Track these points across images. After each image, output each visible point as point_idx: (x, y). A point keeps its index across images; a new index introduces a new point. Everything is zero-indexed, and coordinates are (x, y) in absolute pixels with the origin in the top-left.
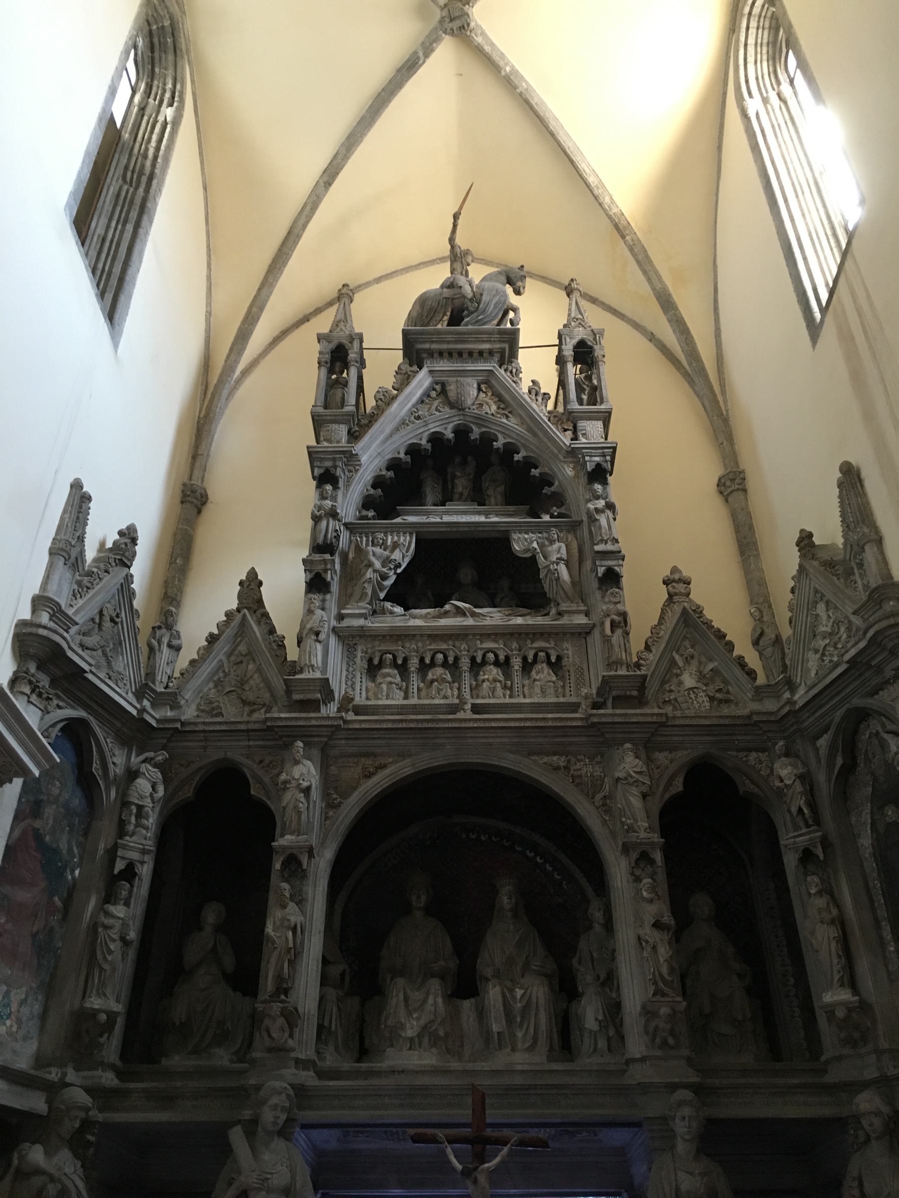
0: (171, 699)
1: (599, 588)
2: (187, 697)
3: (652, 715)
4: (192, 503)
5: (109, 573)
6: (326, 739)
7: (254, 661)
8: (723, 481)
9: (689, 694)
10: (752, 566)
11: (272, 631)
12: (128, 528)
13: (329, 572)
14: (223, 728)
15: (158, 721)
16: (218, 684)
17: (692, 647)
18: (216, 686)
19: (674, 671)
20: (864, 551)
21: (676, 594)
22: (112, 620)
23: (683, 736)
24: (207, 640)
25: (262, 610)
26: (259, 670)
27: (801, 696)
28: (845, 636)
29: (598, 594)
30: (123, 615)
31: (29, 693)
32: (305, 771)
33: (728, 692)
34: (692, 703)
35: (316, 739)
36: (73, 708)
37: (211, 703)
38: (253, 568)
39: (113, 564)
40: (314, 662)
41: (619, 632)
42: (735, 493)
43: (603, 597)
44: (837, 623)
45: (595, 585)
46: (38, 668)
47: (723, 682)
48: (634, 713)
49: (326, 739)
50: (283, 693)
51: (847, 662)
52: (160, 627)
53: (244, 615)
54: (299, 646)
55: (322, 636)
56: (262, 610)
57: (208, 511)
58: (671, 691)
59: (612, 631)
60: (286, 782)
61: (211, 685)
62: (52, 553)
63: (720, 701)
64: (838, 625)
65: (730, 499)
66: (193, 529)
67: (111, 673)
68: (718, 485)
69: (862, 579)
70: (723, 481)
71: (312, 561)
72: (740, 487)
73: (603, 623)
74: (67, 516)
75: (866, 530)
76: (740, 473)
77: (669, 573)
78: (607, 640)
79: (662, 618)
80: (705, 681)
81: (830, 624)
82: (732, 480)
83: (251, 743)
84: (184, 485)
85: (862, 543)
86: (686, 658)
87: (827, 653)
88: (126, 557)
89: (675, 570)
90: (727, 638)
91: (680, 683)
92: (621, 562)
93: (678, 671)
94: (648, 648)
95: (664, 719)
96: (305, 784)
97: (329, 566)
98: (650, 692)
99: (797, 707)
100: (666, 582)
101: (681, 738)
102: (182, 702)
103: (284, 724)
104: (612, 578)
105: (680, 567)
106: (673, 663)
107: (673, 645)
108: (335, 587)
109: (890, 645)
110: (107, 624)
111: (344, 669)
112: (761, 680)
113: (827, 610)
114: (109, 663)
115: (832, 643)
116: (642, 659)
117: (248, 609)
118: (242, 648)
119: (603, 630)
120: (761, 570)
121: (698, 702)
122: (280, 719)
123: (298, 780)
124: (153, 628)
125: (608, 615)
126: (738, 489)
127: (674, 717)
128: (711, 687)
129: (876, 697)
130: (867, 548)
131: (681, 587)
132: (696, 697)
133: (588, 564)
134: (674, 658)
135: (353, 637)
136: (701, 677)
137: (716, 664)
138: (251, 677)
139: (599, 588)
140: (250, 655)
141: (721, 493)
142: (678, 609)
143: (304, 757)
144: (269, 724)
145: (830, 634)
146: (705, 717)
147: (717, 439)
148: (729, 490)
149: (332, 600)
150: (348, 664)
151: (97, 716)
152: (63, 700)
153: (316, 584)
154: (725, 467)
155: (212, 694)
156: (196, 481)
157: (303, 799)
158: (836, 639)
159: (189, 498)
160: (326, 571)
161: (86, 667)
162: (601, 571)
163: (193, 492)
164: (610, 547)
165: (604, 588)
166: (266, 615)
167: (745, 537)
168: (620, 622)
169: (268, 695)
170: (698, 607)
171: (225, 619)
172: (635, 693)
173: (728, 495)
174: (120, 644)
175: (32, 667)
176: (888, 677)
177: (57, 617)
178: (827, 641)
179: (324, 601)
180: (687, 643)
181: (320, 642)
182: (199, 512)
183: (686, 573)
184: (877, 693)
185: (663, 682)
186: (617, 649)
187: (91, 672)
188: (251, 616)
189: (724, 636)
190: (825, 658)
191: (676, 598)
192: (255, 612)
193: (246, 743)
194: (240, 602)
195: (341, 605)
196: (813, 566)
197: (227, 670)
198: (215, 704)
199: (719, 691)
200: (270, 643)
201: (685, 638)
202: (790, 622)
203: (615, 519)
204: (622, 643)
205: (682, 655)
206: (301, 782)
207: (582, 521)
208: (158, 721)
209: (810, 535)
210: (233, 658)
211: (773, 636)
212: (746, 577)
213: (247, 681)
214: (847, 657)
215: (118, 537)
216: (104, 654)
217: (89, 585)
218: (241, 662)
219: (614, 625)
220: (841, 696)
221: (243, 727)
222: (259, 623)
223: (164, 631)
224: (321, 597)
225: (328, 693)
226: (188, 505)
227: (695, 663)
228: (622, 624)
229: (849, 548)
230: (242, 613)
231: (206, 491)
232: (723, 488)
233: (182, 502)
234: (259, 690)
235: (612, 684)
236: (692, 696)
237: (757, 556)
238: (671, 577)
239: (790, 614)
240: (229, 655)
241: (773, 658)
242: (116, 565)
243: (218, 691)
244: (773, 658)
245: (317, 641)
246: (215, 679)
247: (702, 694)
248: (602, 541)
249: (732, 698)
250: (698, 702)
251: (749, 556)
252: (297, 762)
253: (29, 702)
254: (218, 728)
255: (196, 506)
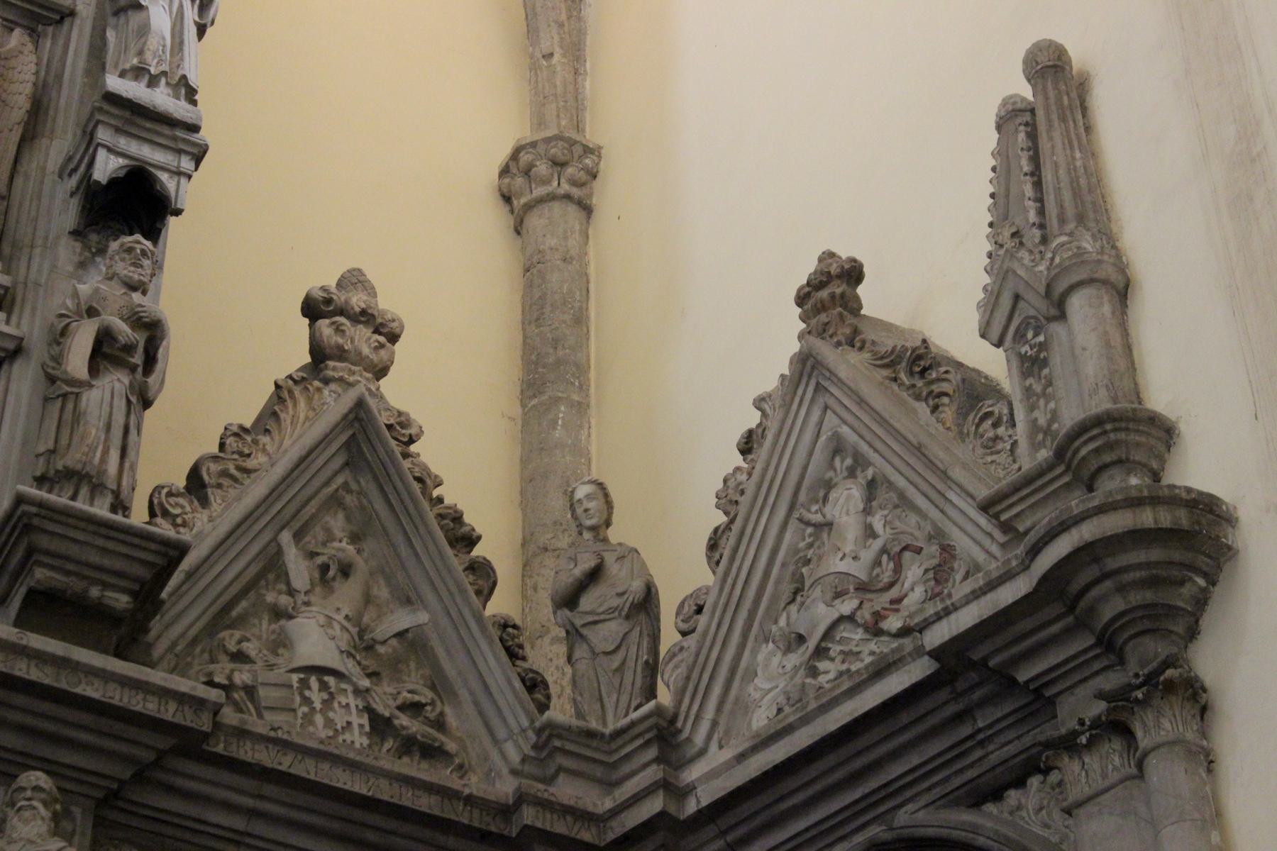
1: (76, 234)
3: (165, 693)
8: (525, 158)
9: (304, 684)
10: (558, 433)
17: (355, 538)
19: (270, 598)
20: (1062, 316)
21: (341, 354)
23: (254, 814)
27: (712, 773)
28: (918, 594)
29: (67, 251)
33: (440, 724)
34: (308, 719)
41: (116, 382)
42: (557, 207)
43: (82, 265)
44: (897, 555)
45: (67, 213)
47: (433, 688)
48: (93, 668)
51: (936, 654)
58: (240, 657)
59: (94, 370)
63: (409, 745)
64: (897, 560)
65: (535, 221)
68: (505, 171)
69: (1032, 408)
70: (525, 158)
72: (576, 192)
73: (60, 336)
75: (1088, 244)
76: (588, 150)
77: (332, 283)
78: (59, 391)
79: (270, 416)
80: (371, 664)
81: (867, 556)
82: (558, 164)
85: (1061, 286)
86: (325, 568)
87: (835, 649)
89: (354, 279)
90: (477, 551)
91: (281, 643)
92: (186, 164)
93: (284, 600)
94: (196, 484)
95: (204, 723)
98: (169, 631)
99: (691, 807)
100: (313, 309)
101: (238, 823)
104: (134, 207)
105: (371, 275)
106: (273, 566)
107: (288, 509)
109: (1107, 613)
112: (561, 712)
113: (867, 511)
115: (865, 615)
116: (166, 513)
119: (58, 360)
120: (581, 452)
121: (329, 723)
125: (92, 312)
126: (568, 197)
127: (242, 733)
128: (387, 688)
129: (990, 808)
130: (1078, 304)
131: (361, 339)
132: (327, 703)
133: (56, 147)
134: (279, 552)
136: (363, 645)
137: (423, 617)
139: (76, 234)
141: (507, 199)
142: (335, 404)
145: (862, 588)
146: (353, 766)
147: (532, 32)
148: (539, 191)
154: (540, 123)
158: (883, 600)
162: (106, 167)
164: (161, 98)
165: (94, 237)
167: (556, 343)
168: (129, 348)
170: (403, 421)
172: (121, 601)
173: (528, 207)
176: (1073, 724)
178: (846, 607)
180: (337, 523)
183: (387, 303)
184: (996, 795)
185: (222, 618)
186: (93, 430)
189: (470, 540)
190: (822, 665)
191: (334, 368)
196: (848, 365)
199: (414, 708)
201: (335, 502)
202: (713, 546)
203: (201, 30)
204: (119, 419)
205: (312, 555)
207: (72, 14)
209: (854, 273)
211: (637, 586)
212: (525, 461)
214: (938, 635)
219: (105, 351)
220: (858, 793)
227: (347, 595)
228: (138, 359)
229: (1006, 302)
232: (520, 181)
235: (43, 541)
236: (317, 697)
237: (581, 408)
238: (340, 298)
239: (721, 519)
241: (616, 661)
244: (616, 661)
247: (352, 700)
248: (139, 72)
249: (451, 746)
250: (329, 723)
251: (556, 401)
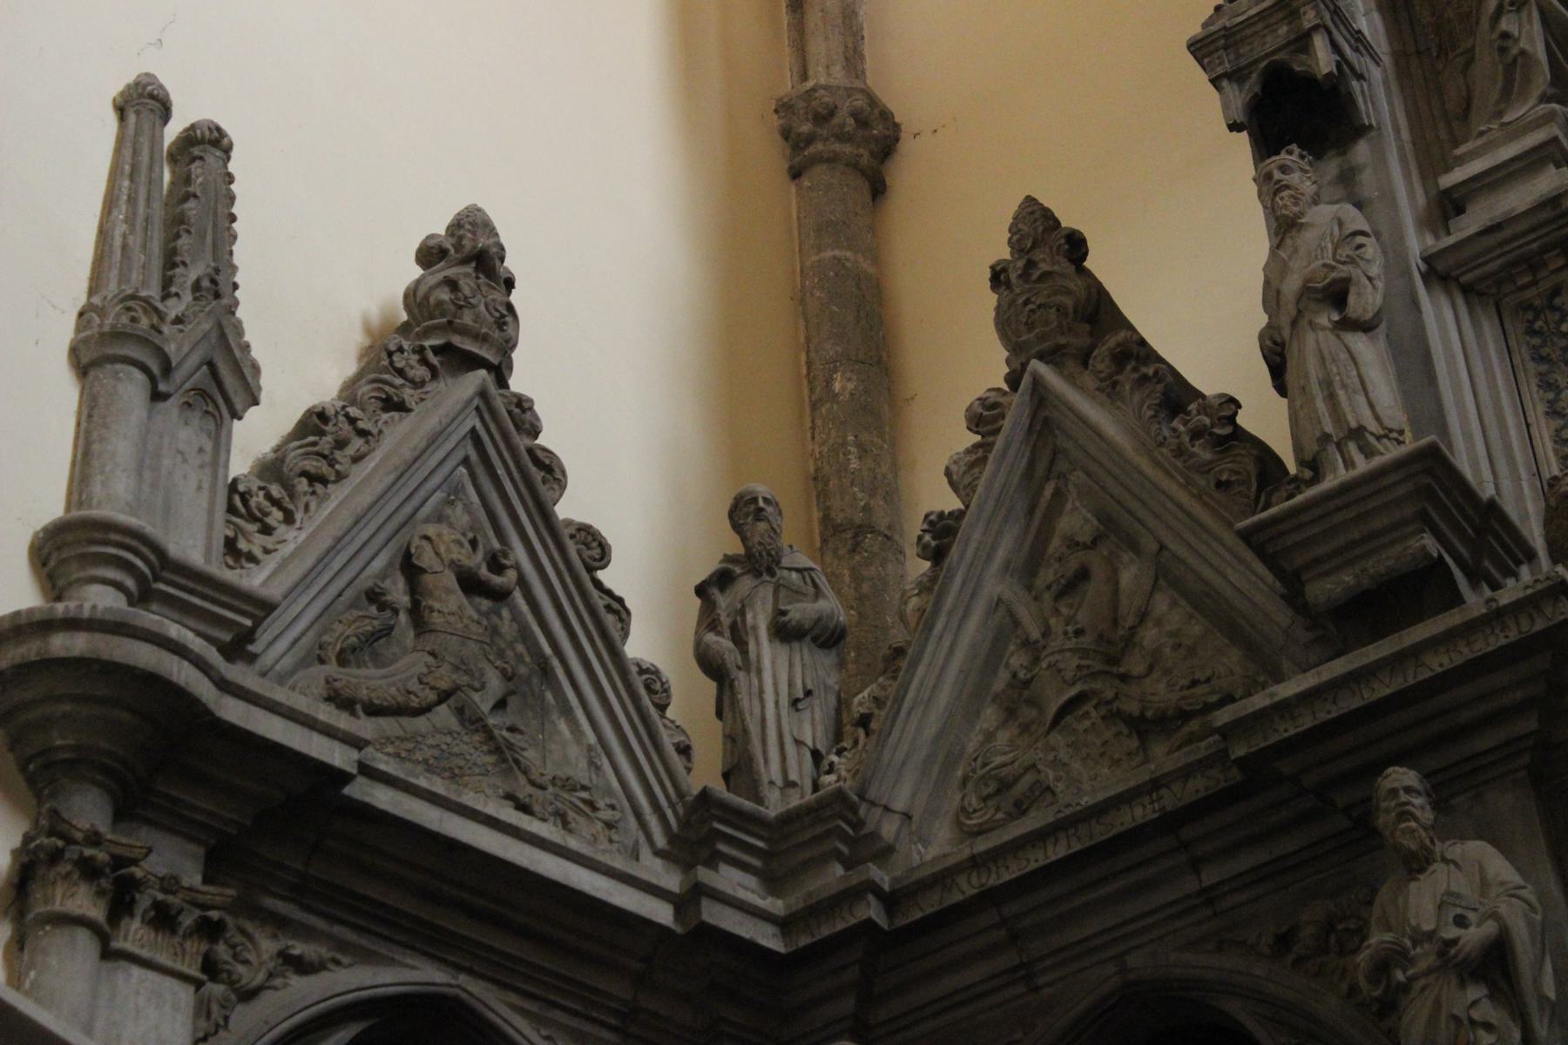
0: (835, 822)
2: (899, 804)
4: (832, 159)
5: (401, 407)
6: (1530, 724)
7: (1134, 546)
11: (1176, 395)
12: (456, 226)
13: (1320, 43)
14: (1058, 851)
15: (785, 925)
16: (1018, 699)
18: (1010, 713)
22: (470, 584)
24: (925, 552)
25: (1112, 341)
26: (1165, 573)
30: (520, 553)
31: (97, 913)
32: (1462, 884)
35: (1483, 742)
36: (367, 957)
37: (1005, 786)
38: (1030, 201)
39: (420, 372)
40: (1358, 413)
46: (122, 814)
49: (1530, 724)
50: (1282, 616)
52: (722, 579)
53: (1037, 382)
54: (1281, 388)
55: (1365, 301)
56: (1112, 341)
57: (911, 174)
60: (1382, 967)
61: (990, 715)
62: (91, 358)
66: (875, 261)
67: (524, 791)
71: (1227, 33)
74: (120, 215)
83: (1210, 876)
84: (784, 108)
88: (464, 331)
96: (1474, 936)
97: (1309, 18)
102: (889, 829)
103: (1307, 722)
108: (1379, 98)
110: (448, 600)
111: (1537, 411)
114: (505, 756)
117: (1052, 356)
118: (1075, 521)
122: (1284, 708)
123: (1430, 935)
124: (701, 590)
135: (1532, 263)
138: (1143, 616)
140: (1113, 530)
143: (1447, 828)
144: (1239, 751)
149: (1387, 158)
150: (1546, 384)
151: (501, 972)
152: (308, 933)
153: (1290, 112)
155: (1006, 749)
156: (827, 73)
157: (1487, 1011)
159: (819, 146)
160: (1302, 42)
161: (338, 756)
163: (823, 117)
166: (1137, 353)
169: (1233, 658)
171: (978, 438)
174: (545, 671)
175: (88, 810)
177: (168, 600)
179: (1347, 178)
181: (1366, 327)
182: (878, 188)
187: (366, 770)
188: (1071, 379)
192: (1085, 359)
193: (1190, 885)
194: (1017, 350)
195: (1431, 157)
197: (1035, 634)
198: (1029, 779)
200: (1180, 452)
206: (1451, 932)
208: (785, 925)
210: (1047, 575)
213: (1130, 641)
215: (418, 272)
216: (471, 721)
217: (312, 465)
218: (1083, 574)
221: (1140, 813)
222: (1110, 390)
223: (745, 585)
224: (1332, 167)
225: (1486, 526)
226: (820, 173)
230: (1026, 380)
231: (873, 101)
233: (795, 174)
234: (1191, 652)
240: (1028, 568)
242: (435, 375)
243: (1025, 728)
245: (1349, 324)
246: (1000, 682)
252: (1417, 864)
253: (109, 954)
254: (1038, 858)
255: (854, 166)
